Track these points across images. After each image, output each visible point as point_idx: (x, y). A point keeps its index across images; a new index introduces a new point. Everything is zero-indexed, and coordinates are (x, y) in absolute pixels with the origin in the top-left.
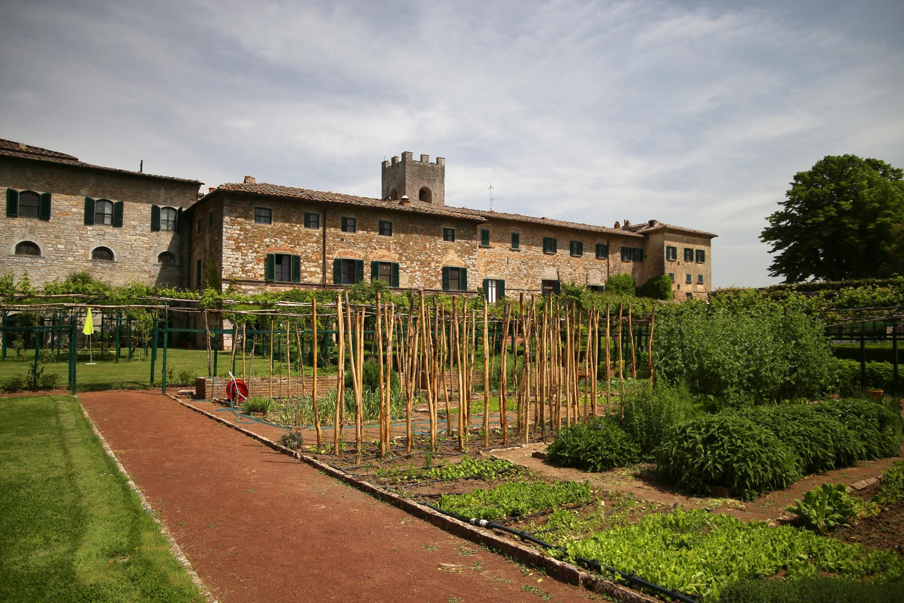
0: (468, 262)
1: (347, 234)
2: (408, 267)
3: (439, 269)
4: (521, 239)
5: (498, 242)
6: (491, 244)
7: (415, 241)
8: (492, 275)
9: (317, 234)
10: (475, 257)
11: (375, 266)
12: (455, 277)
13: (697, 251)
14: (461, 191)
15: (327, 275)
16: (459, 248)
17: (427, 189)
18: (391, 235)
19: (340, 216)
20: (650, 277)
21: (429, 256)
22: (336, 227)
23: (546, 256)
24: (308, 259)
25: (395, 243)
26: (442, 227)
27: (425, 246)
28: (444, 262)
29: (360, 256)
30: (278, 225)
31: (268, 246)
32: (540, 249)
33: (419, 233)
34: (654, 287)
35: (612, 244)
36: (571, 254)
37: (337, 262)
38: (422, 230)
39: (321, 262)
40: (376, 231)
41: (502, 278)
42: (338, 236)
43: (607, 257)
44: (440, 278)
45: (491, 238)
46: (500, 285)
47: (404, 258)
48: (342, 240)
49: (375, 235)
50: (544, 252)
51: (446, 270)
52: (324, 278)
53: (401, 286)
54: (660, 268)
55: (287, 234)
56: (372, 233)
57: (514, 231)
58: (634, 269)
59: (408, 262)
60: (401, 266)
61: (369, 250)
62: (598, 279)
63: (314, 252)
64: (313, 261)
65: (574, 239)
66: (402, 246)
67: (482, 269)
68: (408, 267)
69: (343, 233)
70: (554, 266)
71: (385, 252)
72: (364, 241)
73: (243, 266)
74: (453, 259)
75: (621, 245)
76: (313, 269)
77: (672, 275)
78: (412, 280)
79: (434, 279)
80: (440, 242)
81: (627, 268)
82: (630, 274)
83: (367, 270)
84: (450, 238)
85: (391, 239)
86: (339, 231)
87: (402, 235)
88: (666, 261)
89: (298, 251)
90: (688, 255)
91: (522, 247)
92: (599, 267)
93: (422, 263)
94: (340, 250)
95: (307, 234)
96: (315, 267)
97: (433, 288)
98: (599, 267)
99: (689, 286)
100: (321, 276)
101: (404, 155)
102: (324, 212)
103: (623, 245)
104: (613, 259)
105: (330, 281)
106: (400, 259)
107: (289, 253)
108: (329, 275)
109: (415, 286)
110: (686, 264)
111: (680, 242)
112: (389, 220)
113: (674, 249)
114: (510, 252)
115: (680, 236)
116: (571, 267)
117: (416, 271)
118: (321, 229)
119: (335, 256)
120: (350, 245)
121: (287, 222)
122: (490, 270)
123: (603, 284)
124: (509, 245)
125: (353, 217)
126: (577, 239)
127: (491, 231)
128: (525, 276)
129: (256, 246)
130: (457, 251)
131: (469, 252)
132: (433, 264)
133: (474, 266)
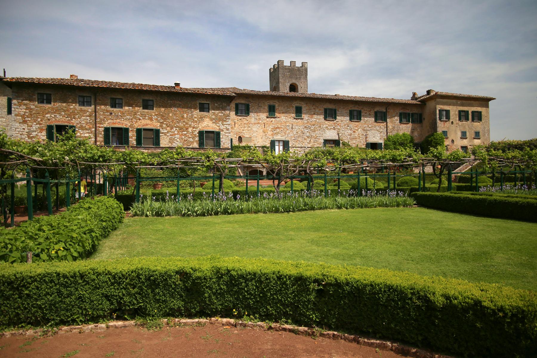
0: (222, 127)
1: (115, 110)
2: (168, 132)
3: (196, 133)
4: (304, 110)
5: (283, 113)
6: (277, 115)
7: (174, 113)
8: (278, 137)
9: (90, 110)
10: (228, 123)
11: (139, 131)
12: (210, 138)
13: (473, 112)
14: (315, 85)
15: (98, 139)
16: (213, 117)
17: (296, 84)
20: (427, 135)
22: (105, 105)
23: (326, 122)
24: (82, 128)
25: (156, 115)
26: (198, 102)
27: (183, 117)
28: (200, 127)
29: (126, 125)
31: (49, 120)
32: (322, 117)
33: (178, 107)
34: (427, 143)
35: (391, 111)
36: (351, 120)
37: (107, 130)
39: (94, 129)
40: (140, 107)
41: (287, 139)
42: (107, 111)
44: (197, 139)
45: (277, 111)
46: (286, 144)
47: (164, 126)
48: (111, 114)
49: (139, 110)
50: (325, 119)
51: (201, 133)
52: (96, 141)
53: (161, 146)
54: (434, 127)
55: (65, 111)
56: (137, 108)
57: (298, 105)
58: (413, 130)
59: (168, 128)
60: (162, 131)
61: (134, 120)
62: (377, 137)
63: (87, 123)
64: (86, 129)
65: (353, 109)
66: (162, 117)
67: (270, 133)
68: (168, 132)
69: (112, 109)
70: (334, 129)
71: (149, 122)
72: (129, 113)
73: (29, 134)
75: (399, 111)
76: (87, 135)
78: (171, 141)
79: (191, 140)
80: (197, 113)
81: (406, 129)
82: (409, 133)
85: (154, 112)
86: (109, 108)
87: (163, 109)
88: (438, 121)
89: (74, 122)
90: (463, 116)
91: (305, 117)
92: (378, 128)
93: (181, 129)
95: (81, 110)
96: (89, 133)
97: (191, 147)
98: (378, 128)
100: (94, 139)
101: (278, 62)
102: (95, 95)
103: (401, 111)
104: (391, 122)
106: (161, 126)
107: (66, 124)
108: (100, 138)
109: (174, 145)
111: (454, 105)
112: (151, 99)
113: (448, 112)
114: (294, 120)
116: (351, 130)
117: (175, 134)
118: (93, 106)
119: (105, 126)
120: (117, 117)
121: (64, 102)
122: (277, 134)
123: (382, 142)
124: (294, 115)
125: (121, 97)
126: (356, 109)
127: (277, 105)
128: (308, 137)
129: (39, 120)
130: (211, 119)
131: (223, 120)
132: (190, 130)
133: (228, 130)
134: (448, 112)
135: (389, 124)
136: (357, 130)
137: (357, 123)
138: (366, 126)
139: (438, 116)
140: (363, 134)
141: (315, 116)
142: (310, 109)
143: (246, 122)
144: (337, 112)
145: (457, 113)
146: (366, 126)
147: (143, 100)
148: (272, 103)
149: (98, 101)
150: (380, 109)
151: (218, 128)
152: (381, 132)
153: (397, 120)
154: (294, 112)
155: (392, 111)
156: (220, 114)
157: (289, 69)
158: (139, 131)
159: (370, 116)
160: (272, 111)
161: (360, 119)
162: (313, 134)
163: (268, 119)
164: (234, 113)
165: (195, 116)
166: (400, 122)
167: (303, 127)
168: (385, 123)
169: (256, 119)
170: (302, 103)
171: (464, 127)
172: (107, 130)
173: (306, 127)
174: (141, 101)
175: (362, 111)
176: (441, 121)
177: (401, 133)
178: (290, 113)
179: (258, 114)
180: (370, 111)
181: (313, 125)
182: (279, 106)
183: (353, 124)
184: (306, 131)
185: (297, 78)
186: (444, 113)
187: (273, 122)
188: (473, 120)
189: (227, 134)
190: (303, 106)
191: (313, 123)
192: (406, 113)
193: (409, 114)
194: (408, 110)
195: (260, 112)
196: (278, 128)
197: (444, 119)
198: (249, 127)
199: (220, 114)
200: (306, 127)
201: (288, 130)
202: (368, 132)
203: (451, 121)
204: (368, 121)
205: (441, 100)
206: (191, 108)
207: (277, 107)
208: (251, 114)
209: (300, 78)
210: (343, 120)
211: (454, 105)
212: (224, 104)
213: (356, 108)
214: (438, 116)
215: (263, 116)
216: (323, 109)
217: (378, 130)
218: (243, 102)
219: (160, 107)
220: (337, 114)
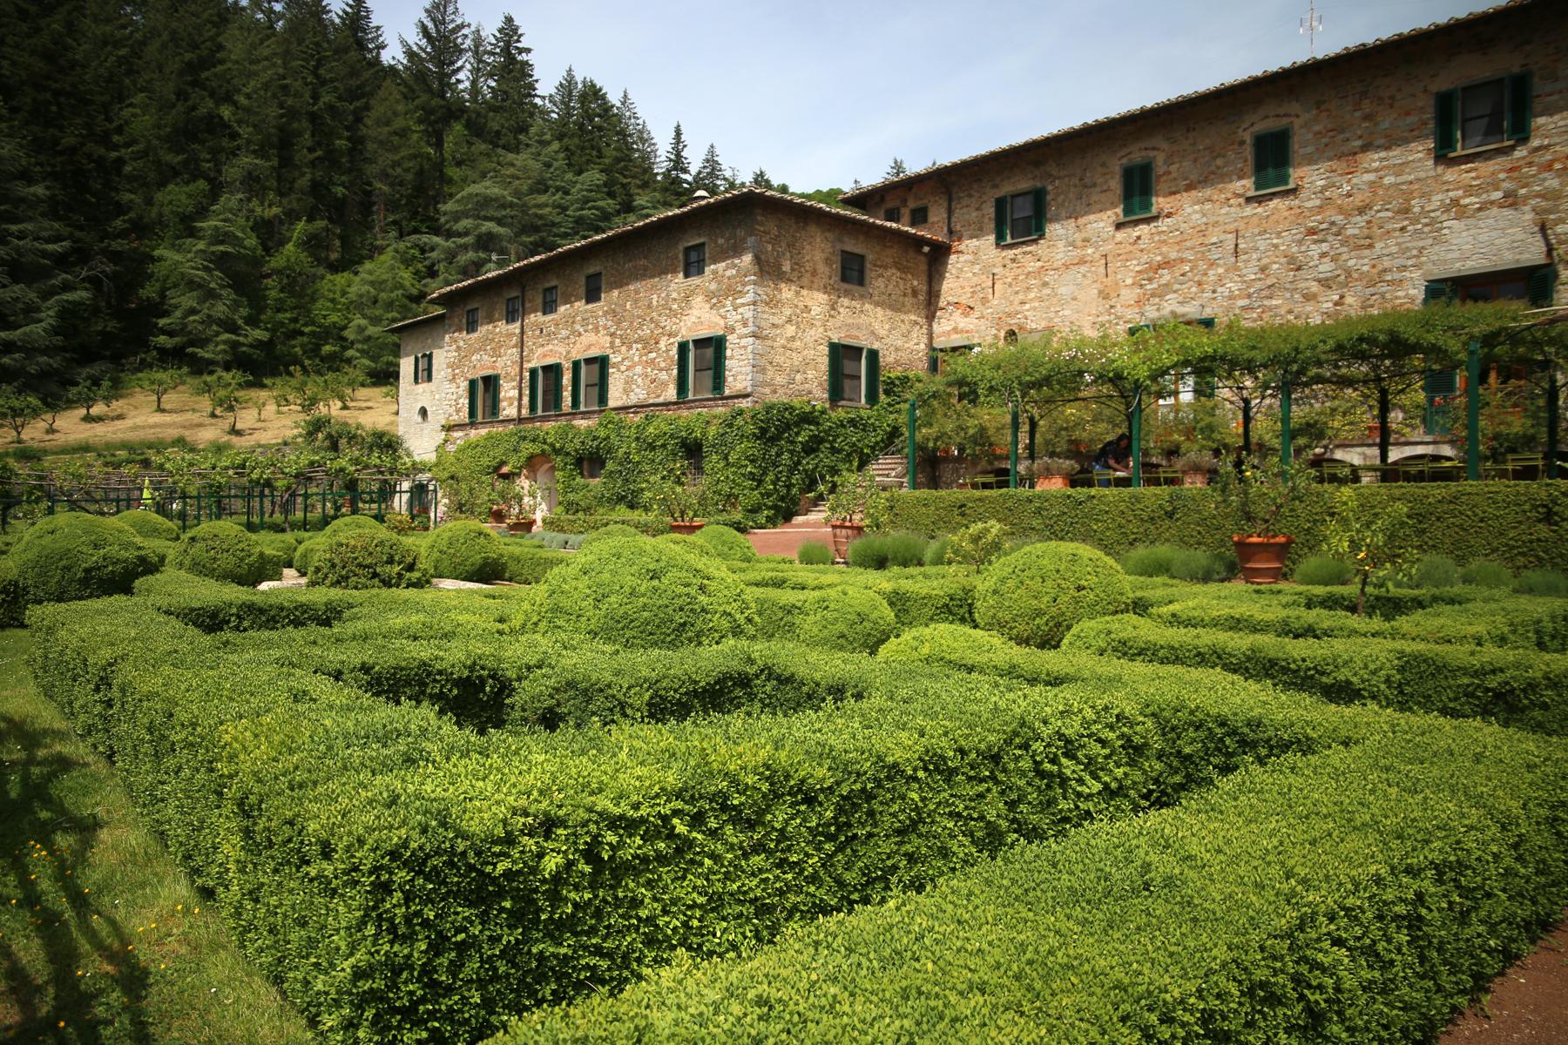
0: (733, 318)
3: (674, 352)
4: (1300, 143)
5: (1189, 188)
6: (1160, 203)
11: (576, 366)
16: (713, 286)
18: (599, 299)
19: (540, 288)
21: (657, 326)
23: (1451, 174)
27: (649, 307)
30: (483, 330)
32: (1419, 153)
37: (533, 372)
38: (646, 269)
45: (1163, 186)
49: (580, 305)
50: (1443, 156)
53: (612, 403)
60: (614, 359)
67: (1129, 295)
74: (700, 320)
79: (664, 376)
80: (677, 283)
83: (567, 379)
84: (693, 270)
87: (616, 293)
91: (1310, 177)
94: (540, 351)
97: (661, 400)
105: (525, 412)
106: (612, 347)
114: (1249, 210)
122: (1160, 294)
124: (1246, 185)
127: (1160, 159)
128: (1326, 283)
130: (709, 296)
131: (732, 291)
132: (662, 345)
141: (1374, 159)
147: (588, 278)
149: (528, 305)
151: (722, 322)
154: (1249, 168)
156: (728, 273)
158: (576, 366)
160: (1137, 195)
162: (1360, 263)
163: (1120, 235)
164: (992, 238)
165: (674, 295)
167: (1298, 233)
169: (1072, 244)
170: (1295, 107)
172: (533, 372)
174: (583, 281)
179: (1081, 221)
181: (1361, 211)
182: (1169, 161)
184: (1315, 250)
189: (744, 342)
190: (1297, 122)
191: (1358, 199)
195: (1089, 208)
196: (1167, 264)
198: (1045, 284)
199: (728, 273)
201: (1212, 264)
206: (666, 273)
207: (1160, 167)
208: (1054, 229)
212: (740, 233)
218: (1024, 185)
219: (611, 287)
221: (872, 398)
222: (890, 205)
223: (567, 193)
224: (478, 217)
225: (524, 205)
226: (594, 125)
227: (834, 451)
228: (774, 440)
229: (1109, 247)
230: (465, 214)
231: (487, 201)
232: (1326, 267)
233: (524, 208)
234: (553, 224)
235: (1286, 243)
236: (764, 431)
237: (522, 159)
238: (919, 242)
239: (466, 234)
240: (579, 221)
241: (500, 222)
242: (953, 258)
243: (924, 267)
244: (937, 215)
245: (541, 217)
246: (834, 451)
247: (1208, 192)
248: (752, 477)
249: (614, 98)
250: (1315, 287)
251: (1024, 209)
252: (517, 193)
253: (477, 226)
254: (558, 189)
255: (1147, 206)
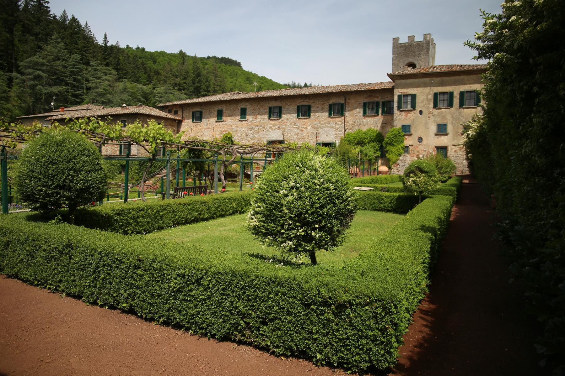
4: (248, 111)
5: (229, 116)
6: (224, 118)
23: (271, 122)
36: (298, 116)
43: (342, 115)
45: (224, 115)
70: (279, 128)
77: (406, 129)
79: (116, 149)
81: (373, 124)
92: (333, 125)
98: (333, 125)
99: (443, 137)
103: (366, 101)
104: (352, 116)
110: (436, 112)
114: (240, 123)
115: (427, 80)
116: (298, 128)
124: (239, 118)
128: (251, 139)
134: (414, 97)
135: (347, 119)
136: (306, 128)
137: (305, 120)
138: (317, 122)
139: (396, 105)
140: (313, 133)
141: (259, 117)
142: (254, 110)
143: (200, 128)
144: (283, 109)
145: (431, 97)
146: (317, 122)
148: (220, 107)
150: (336, 101)
152: (337, 130)
153: (359, 113)
155: (353, 101)
157: (405, 46)
159: (323, 110)
160: (220, 115)
161: (309, 116)
163: (217, 124)
166: (364, 115)
168: (343, 118)
170: (247, 104)
171: (444, 117)
173: (250, 129)
175: (312, 105)
176: (401, 111)
177: (364, 129)
178: (235, 115)
180: (323, 105)
181: (258, 126)
183: (303, 122)
185: (415, 56)
186: (409, 99)
187: (221, 126)
188: (461, 105)
191: (257, 124)
192: (373, 102)
193: (377, 104)
194: (378, 97)
195: (211, 117)
197: (409, 107)
200: (250, 129)
202: (320, 130)
203: (418, 109)
204: (320, 117)
205: (403, 81)
207: (224, 111)
208: (204, 120)
209: (419, 54)
210: (289, 118)
211: (425, 85)
213: (305, 103)
214: (396, 105)
215: (213, 120)
216: (268, 108)
217: (332, 127)
218: (198, 109)
220: (283, 112)
221: (164, 155)
222: (169, 109)
223: (67, 61)
224: (34, 69)
225: (52, 65)
226: (73, 33)
227: (155, 167)
228: (142, 165)
229: (214, 126)
230: (29, 67)
231: (37, 63)
232: (252, 136)
233: (52, 66)
234: (62, 72)
235: (245, 130)
236: (140, 164)
237: (49, 48)
238: (175, 120)
239: (30, 74)
240: (72, 72)
241: (43, 71)
242: (183, 123)
243: (176, 125)
244: (180, 113)
245: (58, 70)
246: (155, 167)
247: (233, 118)
248: (137, 173)
249: (83, 23)
250: (250, 139)
251: (198, 115)
252: (49, 61)
253: (34, 72)
254: (64, 60)
255: (221, 119)
